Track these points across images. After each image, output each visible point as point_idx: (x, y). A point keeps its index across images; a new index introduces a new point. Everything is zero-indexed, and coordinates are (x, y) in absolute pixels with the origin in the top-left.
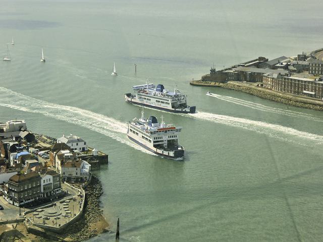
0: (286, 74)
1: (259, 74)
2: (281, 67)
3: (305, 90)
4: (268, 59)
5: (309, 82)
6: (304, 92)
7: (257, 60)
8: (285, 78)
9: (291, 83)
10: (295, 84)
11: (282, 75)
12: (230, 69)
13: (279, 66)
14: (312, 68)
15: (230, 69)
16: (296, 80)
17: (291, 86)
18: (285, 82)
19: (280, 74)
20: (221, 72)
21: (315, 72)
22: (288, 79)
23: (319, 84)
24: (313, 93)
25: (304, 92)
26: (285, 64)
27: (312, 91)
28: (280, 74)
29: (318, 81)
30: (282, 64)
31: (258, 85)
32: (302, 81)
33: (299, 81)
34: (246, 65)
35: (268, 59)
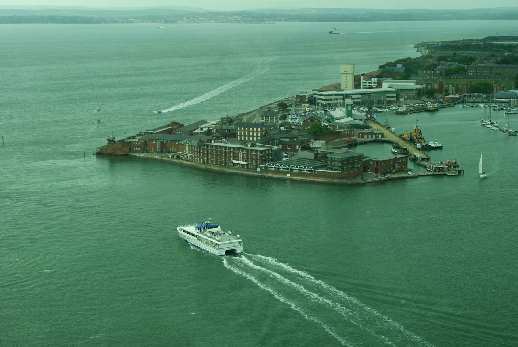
0: (208, 140)
1: (173, 141)
2: (201, 133)
3: (234, 159)
4: (183, 125)
5: (238, 149)
6: (234, 161)
7: (169, 126)
8: (208, 146)
9: (216, 151)
10: (221, 152)
11: (203, 142)
12: (133, 138)
13: (198, 133)
14: (241, 133)
15: (133, 138)
16: (222, 147)
17: (216, 155)
18: (208, 150)
19: (200, 140)
20: (122, 142)
21: (245, 138)
22: (212, 146)
23: (252, 151)
24: (245, 163)
25: (234, 161)
26: (205, 129)
27: (243, 161)
28: (200, 140)
29: (250, 146)
30: (202, 129)
31: (173, 157)
32: (230, 148)
33: (225, 148)
34: (155, 132)
35: (183, 125)
